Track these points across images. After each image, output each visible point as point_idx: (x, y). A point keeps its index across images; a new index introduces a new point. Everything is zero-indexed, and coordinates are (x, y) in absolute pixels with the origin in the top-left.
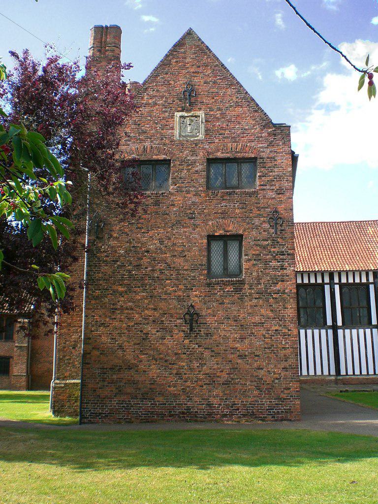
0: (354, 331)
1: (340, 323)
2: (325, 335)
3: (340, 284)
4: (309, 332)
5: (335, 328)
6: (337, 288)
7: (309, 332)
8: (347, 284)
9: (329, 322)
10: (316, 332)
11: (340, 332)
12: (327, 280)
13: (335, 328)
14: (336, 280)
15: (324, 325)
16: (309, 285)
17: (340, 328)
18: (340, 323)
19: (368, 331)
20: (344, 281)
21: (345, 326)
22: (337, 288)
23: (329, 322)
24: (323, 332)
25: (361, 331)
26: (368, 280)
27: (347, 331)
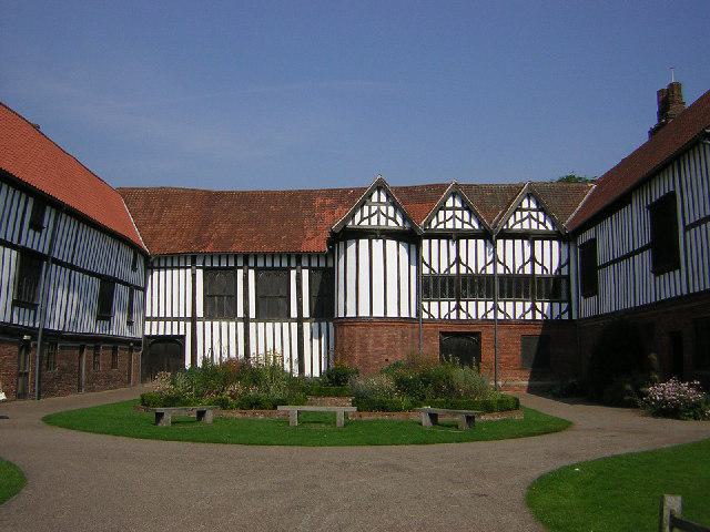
0: (269, 325)
1: (252, 315)
2: (235, 329)
5: (246, 320)
7: (216, 324)
9: (240, 314)
10: (224, 324)
11: (252, 325)
12: (240, 263)
13: (246, 320)
15: (232, 316)
16: (220, 268)
17: (253, 320)
18: (252, 315)
19: (286, 325)
21: (258, 319)
23: (240, 314)
24: (232, 324)
25: (278, 325)
26: (289, 264)
27: (261, 325)
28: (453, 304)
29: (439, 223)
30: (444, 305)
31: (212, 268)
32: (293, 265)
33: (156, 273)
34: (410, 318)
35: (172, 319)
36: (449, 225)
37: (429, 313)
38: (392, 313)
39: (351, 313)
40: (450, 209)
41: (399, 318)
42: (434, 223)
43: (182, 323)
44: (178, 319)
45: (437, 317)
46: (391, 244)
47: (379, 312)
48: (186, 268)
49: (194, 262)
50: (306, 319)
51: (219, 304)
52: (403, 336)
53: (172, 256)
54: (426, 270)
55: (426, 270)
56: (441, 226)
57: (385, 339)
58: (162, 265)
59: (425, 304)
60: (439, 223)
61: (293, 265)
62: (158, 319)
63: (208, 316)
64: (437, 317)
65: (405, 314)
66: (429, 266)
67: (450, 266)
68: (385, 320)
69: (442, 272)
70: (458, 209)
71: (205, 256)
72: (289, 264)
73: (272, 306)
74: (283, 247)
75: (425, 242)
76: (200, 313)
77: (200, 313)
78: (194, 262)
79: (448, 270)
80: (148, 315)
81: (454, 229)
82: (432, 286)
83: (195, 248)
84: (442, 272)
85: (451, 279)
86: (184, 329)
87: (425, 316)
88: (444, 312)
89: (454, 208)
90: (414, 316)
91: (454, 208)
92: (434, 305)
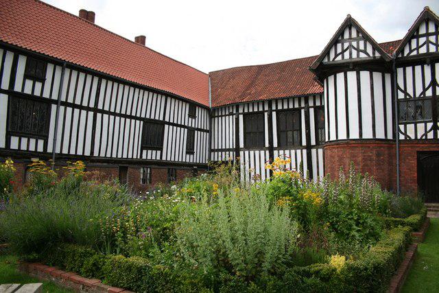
1: (275, 145)
3: (278, 112)
4: (252, 152)
5: (271, 149)
6: (274, 114)
7: (252, 152)
8: (283, 110)
9: (267, 145)
10: (257, 152)
12: (266, 108)
13: (271, 149)
14: (274, 108)
15: (262, 147)
16: (254, 113)
17: (276, 149)
18: (275, 145)
19: (299, 152)
20: (280, 107)
21: (280, 147)
22: (274, 114)
23: (267, 145)
24: (262, 152)
26: (300, 105)
28: (430, 125)
29: (411, 51)
30: (421, 127)
31: (249, 113)
32: (303, 105)
33: (216, 119)
34: (386, 140)
35: (226, 150)
36: (423, 50)
37: (405, 134)
38: (367, 134)
39: (333, 138)
40: (423, 36)
41: (375, 140)
42: (406, 52)
43: (231, 153)
44: (229, 150)
45: (413, 138)
46: (365, 75)
47: (354, 135)
48: (232, 114)
49: (237, 110)
50: (313, 147)
51: (254, 139)
52: (378, 155)
53: (225, 107)
54: (401, 96)
55: (401, 96)
56: (415, 53)
57: (360, 159)
58: (220, 114)
59: (402, 127)
60: (411, 51)
61: (303, 105)
62: (218, 150)
63: (247, 147)
64: (413, 138)
65: (380, 135)
66: (405, 92)
67: (425, 90)
68: (361, 141)
69: (417, 96)
70: (432, 34)
71: (244, 104)
72: (300, 105)
73: (288, 139)
74: (294, 93)
75: (400, 71)
76: (242, 145)
77: (242, 145)
78: (237, 110)
79: (423, 93)
80: (213, 148)
81: (428, 53)
82: (404, 110)
83: (237, 100)
84: (417, 96)
85: (423, 98)
86: (230, 156)
87: (402, 137)
88: (421, 132)
89: (428, 35)
90: (390, 137)
91: (428, 35)
92: (411, 127)
